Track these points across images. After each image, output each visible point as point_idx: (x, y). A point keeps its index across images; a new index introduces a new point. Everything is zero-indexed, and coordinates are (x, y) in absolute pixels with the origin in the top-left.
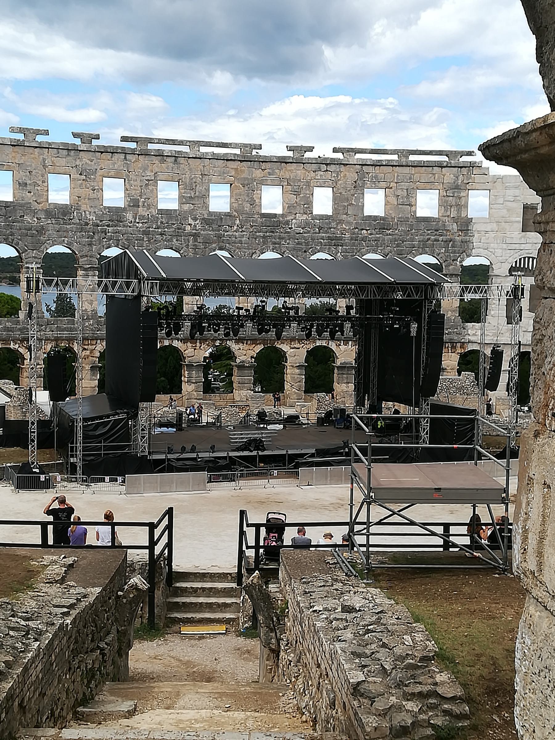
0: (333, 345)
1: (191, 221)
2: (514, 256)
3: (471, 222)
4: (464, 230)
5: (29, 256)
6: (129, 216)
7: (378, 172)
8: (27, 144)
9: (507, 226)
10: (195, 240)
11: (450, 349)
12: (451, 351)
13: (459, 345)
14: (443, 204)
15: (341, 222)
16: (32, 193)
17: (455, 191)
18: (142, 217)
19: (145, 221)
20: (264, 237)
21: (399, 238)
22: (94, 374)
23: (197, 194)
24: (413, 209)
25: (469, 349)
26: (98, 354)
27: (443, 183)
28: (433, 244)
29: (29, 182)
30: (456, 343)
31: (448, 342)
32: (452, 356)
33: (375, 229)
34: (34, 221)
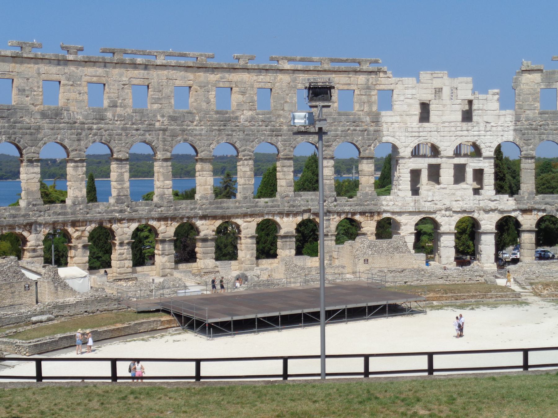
0: (278, 219)
1: (159, 118)
5: (29, 151)
6: (109, 115)
8: (25, 55)
9: (407, 118)
10: (164, 134)
15: (279, 116)
16: (29, 98)
18: (120, 116)
19: (123, 119)
20: (219, 130)
22: (84, 252)
23: (164, 95)
26: (87, 234)
28: (352, 134)
29: (27, 88)
34: (32, 121)
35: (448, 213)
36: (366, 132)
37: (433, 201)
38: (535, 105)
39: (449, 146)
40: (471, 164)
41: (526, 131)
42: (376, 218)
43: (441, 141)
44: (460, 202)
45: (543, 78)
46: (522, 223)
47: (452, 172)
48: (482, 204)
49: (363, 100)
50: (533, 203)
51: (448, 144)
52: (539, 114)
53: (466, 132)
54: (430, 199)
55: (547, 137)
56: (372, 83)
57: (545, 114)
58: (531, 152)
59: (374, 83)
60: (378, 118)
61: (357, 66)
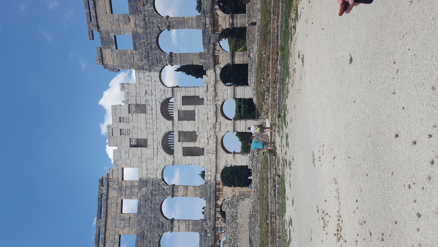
2: (162, 152)
3: (141, 179)
4: (146, 183)
7: (109, 240)
9: (144, 157)
11: (220, 192)
12: (222, 191)
13: (217, 187)
14: (130, 197)
17: (123, 190)
21: (149, 227)
24: (132, 216)
25: (220, 180)
27: (117, 197)
28: (154, 204)
30: (216, 188)
31: (216, 194)
32: (225, 191)
33: (143, 242)
35: (218, 126)
36: (153, 192)
37: (208, 138)
38: (130, 53)
39: (165, 124)
40: (178, 107)
41: (150, 61)
42: (221, 186)
43: (161, 131)
44: (209, 116)
45: (107, 47)
46: (226, 64)
47: (185, 122)
48: (210, 98)
49: (129, 193)
50: (209, 55)
51: (163, 125)
52: (136, 50)
53: (153, 110)
54: (206, 141)
55: (153, 44)
56: (117, 185)
57: (136, 44)
58: (166, 57)
59: (117, 183)
60: (144, 181)
61: (104, 197)
